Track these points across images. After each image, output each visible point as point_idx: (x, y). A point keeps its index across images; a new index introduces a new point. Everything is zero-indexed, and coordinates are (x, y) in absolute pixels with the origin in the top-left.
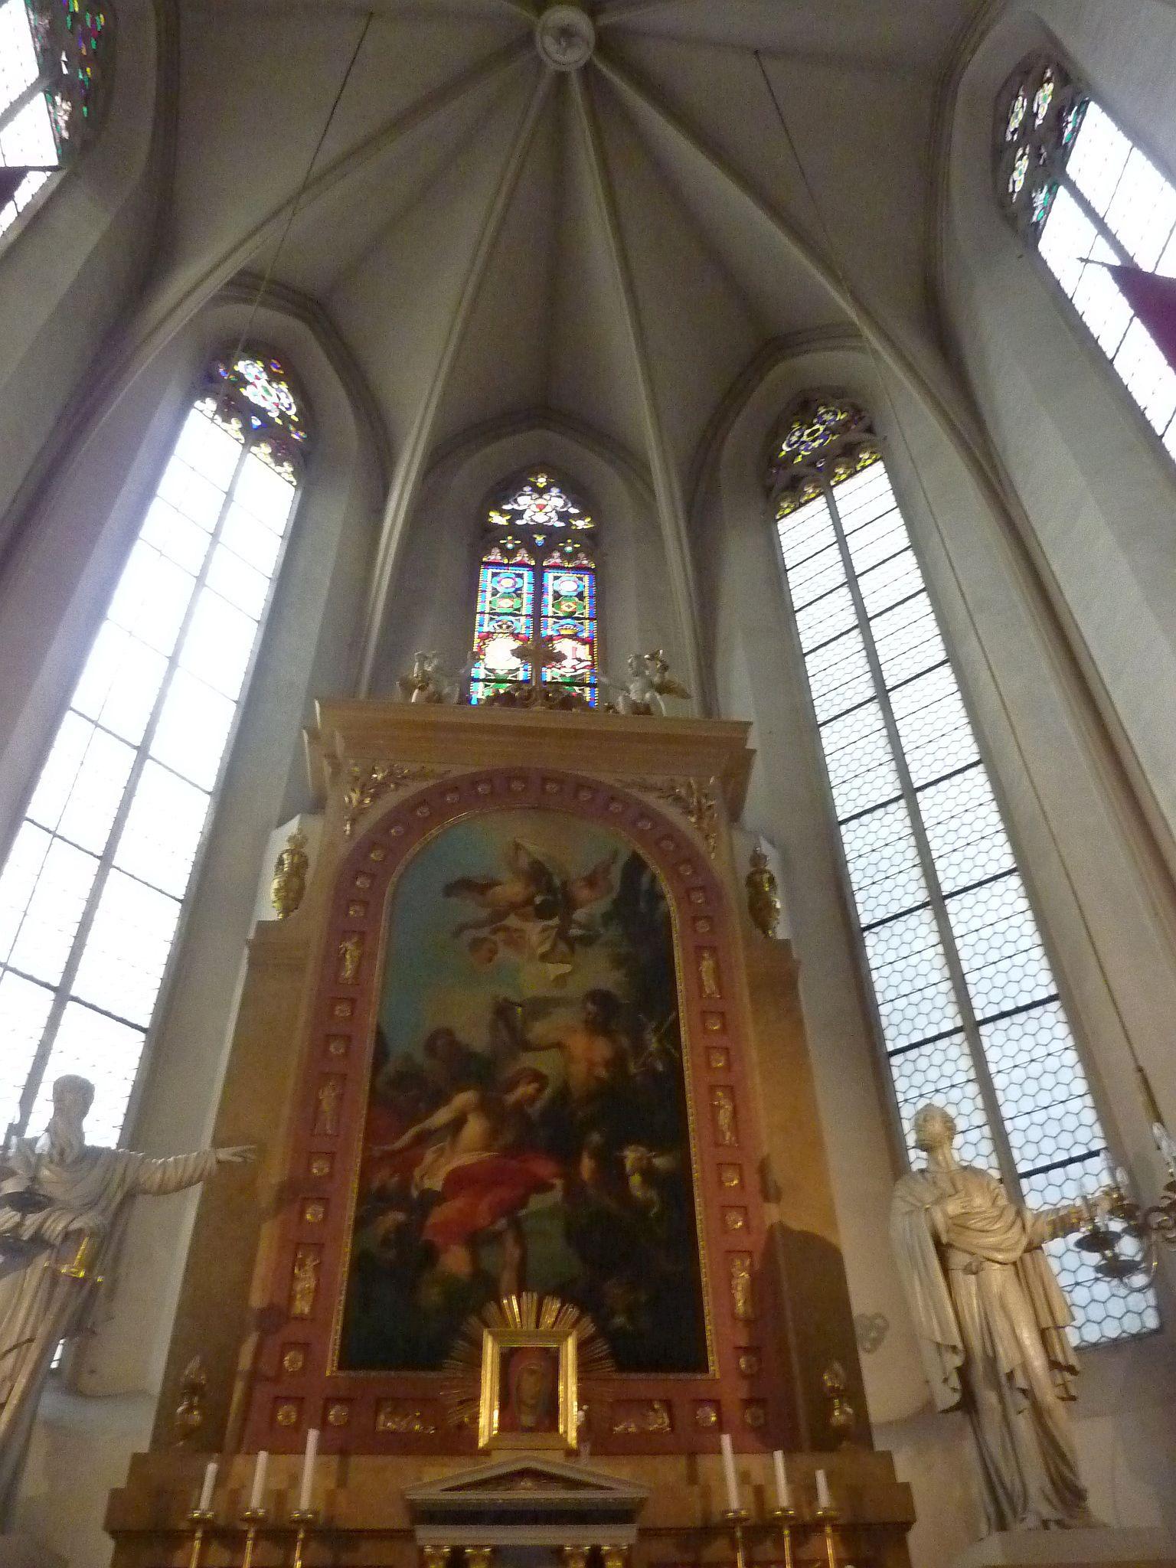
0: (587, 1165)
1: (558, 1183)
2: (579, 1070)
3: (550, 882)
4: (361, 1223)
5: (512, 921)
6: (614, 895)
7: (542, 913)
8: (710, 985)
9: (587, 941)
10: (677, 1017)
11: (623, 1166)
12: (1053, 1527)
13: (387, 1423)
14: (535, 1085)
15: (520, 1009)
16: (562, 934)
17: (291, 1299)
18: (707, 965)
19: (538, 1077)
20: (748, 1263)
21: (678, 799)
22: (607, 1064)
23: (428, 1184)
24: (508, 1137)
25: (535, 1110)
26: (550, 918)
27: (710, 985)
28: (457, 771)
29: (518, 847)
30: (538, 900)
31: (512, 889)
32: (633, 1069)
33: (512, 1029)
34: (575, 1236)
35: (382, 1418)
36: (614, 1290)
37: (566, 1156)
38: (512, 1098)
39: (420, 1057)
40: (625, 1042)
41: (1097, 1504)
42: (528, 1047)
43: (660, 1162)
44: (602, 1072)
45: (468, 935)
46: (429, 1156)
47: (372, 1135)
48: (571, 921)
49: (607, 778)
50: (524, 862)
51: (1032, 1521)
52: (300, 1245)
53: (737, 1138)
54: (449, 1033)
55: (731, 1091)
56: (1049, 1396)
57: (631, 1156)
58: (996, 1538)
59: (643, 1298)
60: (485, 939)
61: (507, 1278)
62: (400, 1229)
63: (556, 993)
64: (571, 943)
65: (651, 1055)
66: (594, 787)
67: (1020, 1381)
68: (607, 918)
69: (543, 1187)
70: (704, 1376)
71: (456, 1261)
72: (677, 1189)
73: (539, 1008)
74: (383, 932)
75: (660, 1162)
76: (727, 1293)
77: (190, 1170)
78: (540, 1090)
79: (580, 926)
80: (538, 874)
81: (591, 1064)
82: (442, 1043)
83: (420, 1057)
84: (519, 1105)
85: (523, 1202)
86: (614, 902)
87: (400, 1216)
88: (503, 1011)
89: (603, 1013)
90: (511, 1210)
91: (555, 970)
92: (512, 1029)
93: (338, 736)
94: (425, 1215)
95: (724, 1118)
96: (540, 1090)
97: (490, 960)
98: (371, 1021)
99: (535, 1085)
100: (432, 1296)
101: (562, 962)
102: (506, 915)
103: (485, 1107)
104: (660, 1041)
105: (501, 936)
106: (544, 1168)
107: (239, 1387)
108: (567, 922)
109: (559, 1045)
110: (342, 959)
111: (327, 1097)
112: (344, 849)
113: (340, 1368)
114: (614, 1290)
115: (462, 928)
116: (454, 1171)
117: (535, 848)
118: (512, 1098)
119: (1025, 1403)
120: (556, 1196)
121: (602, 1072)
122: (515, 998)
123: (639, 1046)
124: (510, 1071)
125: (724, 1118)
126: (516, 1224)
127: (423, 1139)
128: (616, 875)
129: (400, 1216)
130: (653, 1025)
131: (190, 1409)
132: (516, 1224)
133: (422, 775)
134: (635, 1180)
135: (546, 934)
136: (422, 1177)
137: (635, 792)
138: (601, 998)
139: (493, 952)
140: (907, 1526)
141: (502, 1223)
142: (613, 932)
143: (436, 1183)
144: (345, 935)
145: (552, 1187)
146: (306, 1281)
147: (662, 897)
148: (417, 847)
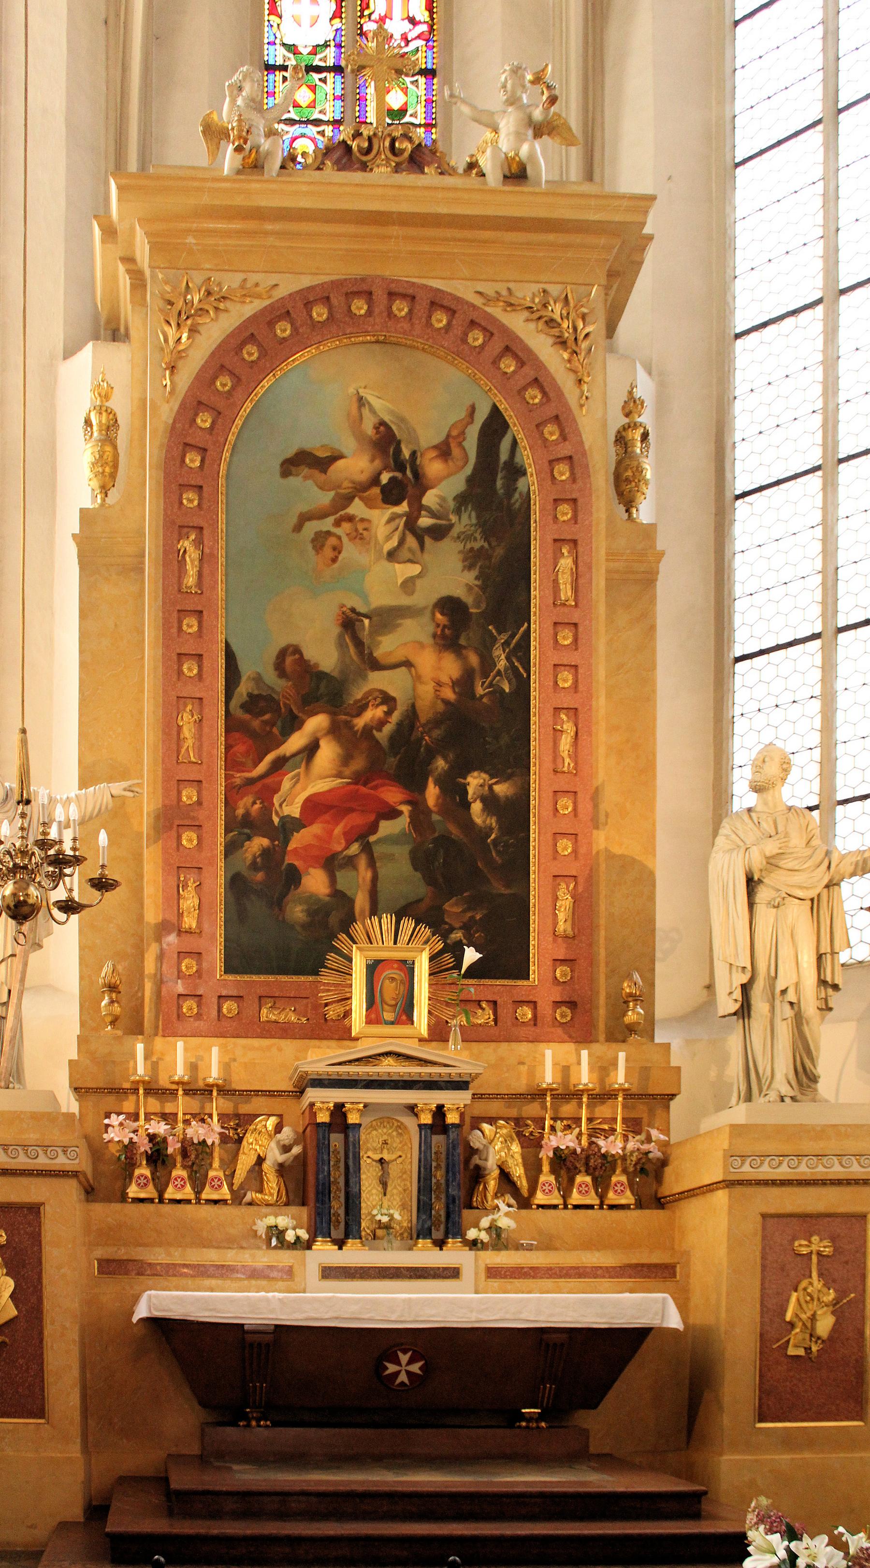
0: (432, 793)
1: (405, 809)
2: (426, 691)
3: (398, 451)
4: (231, 849)
5: (357, 508)
6: (469, 470)
7: (392, 494)
8: (566, 592)
9: (438, 533)
10: (528, 631)
11: (466, 792)
12: (787, 1100)
13: (266, 1014)
14: (384, 708)
15: (366, 622)
16: (411, 525)
17: (180, 915)
18: (566, 563)
19: (388, 700)
20: (572, 886)
21: (551, 323)
22: (455, 684)
23: (287, 810)
24: (358, 764)
25: (383, 735)
26: (397, 503)
27: (566, 592)
28: (289, 285)
29: (361, 401)
30: (385, 478)
31: (357, 465)
32: (480, 691)
33: (359, 644)
34: (421, 860)
35: (264, 1011)
36: (452, 908)
37: (412, 778)
38: (359, 723)
39: (271, 677)
40: (474, 659)
41: (824, 1087)
42: (376, 665)
43: (502, 789)
44: (449, 694)
45: (312, 528)
46: (286, 784)
47: (231, 764)
48: (421, 507)
49: (464, 290)
50: (368, 426)
51: (773, 1096)
52: (180, 868)
53: (576, 764)
54: (297, 650)
55: (574, 712)
56: (810, 1007)
57: (475, 782)
58: (743, 1106)
59: (478, 917)
60: (328, 533)
61: (361, 901)
62: (266, 853)
63: (405, 601)
64: (420, 535)
65: (499, 673)
66: (448, 305)
67: (791, 996)
68: (462, 500)
69: (393, 814)
70: (525, 983)
71: (316, 882)
72: (515, 815)
73: (387, 618)
74: (221, 526)
75: (502, 789)
76: (550, 914)
77: (90, 809)
78: (389, 713)
79: (433, 514)
80: (385, 441)
81: (439, 684)
82: (290, 661)
83: (271, 677)
84: (368, 731)
85: (373, 828)
86: (470, 480)
87: (265, 842)
88: (349, 623)
89: (454, 621)
90: (362, 835)
91: (405, 571)
92: (359, 644)
93: (139, 232)
94: (286, 841)
95: (565, 743)
96: (389, 713)
97: (334, 560)
98: (221, 637)
99: (384, 708)
100: (297, 912)
101: (410, 561)
102: (348, 499)
103: (335, 730)
104: (508, 658)
105: (346, 526)
106: (393, 795)
107: (148, 987)
108: (417, 508)
109: (407, 664)
110: (182, 563)
111: (187, 721)
112: (167, 412)
113: (228, 970)
114: (452, 908)
115: (304, 518)
116: (308, 800)
117: (381, 406)
118: (359, 723)
119: (789, 1012)
120: (402, 823)
121: (449, 694)
122: (362, 609)
123: (487, 663)
124: (358, 694)
125: (565, 743)
126: (367, 848)
127: (280, 764)
128: (471, 443)
129: (265, 842)
130: (503, 638)
131: (112, 1002)
132: (367, 848)
133: (247, 293)
134: (477, 807)
135: (393, 525)
136: (281, 805)
137: (496, 311)
138: (450, 606)
139: (337, 549)
140: (673, 1096)
141: (355, 848)
142: (465, 522)
143: (294, 810)
144: (182, 531)
145: (399, 813)
146: (189, 901)
147: (521, 472)
148: (248, 406)
